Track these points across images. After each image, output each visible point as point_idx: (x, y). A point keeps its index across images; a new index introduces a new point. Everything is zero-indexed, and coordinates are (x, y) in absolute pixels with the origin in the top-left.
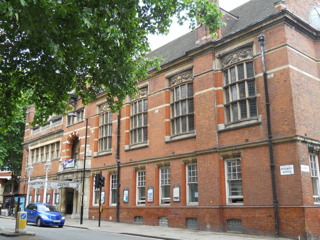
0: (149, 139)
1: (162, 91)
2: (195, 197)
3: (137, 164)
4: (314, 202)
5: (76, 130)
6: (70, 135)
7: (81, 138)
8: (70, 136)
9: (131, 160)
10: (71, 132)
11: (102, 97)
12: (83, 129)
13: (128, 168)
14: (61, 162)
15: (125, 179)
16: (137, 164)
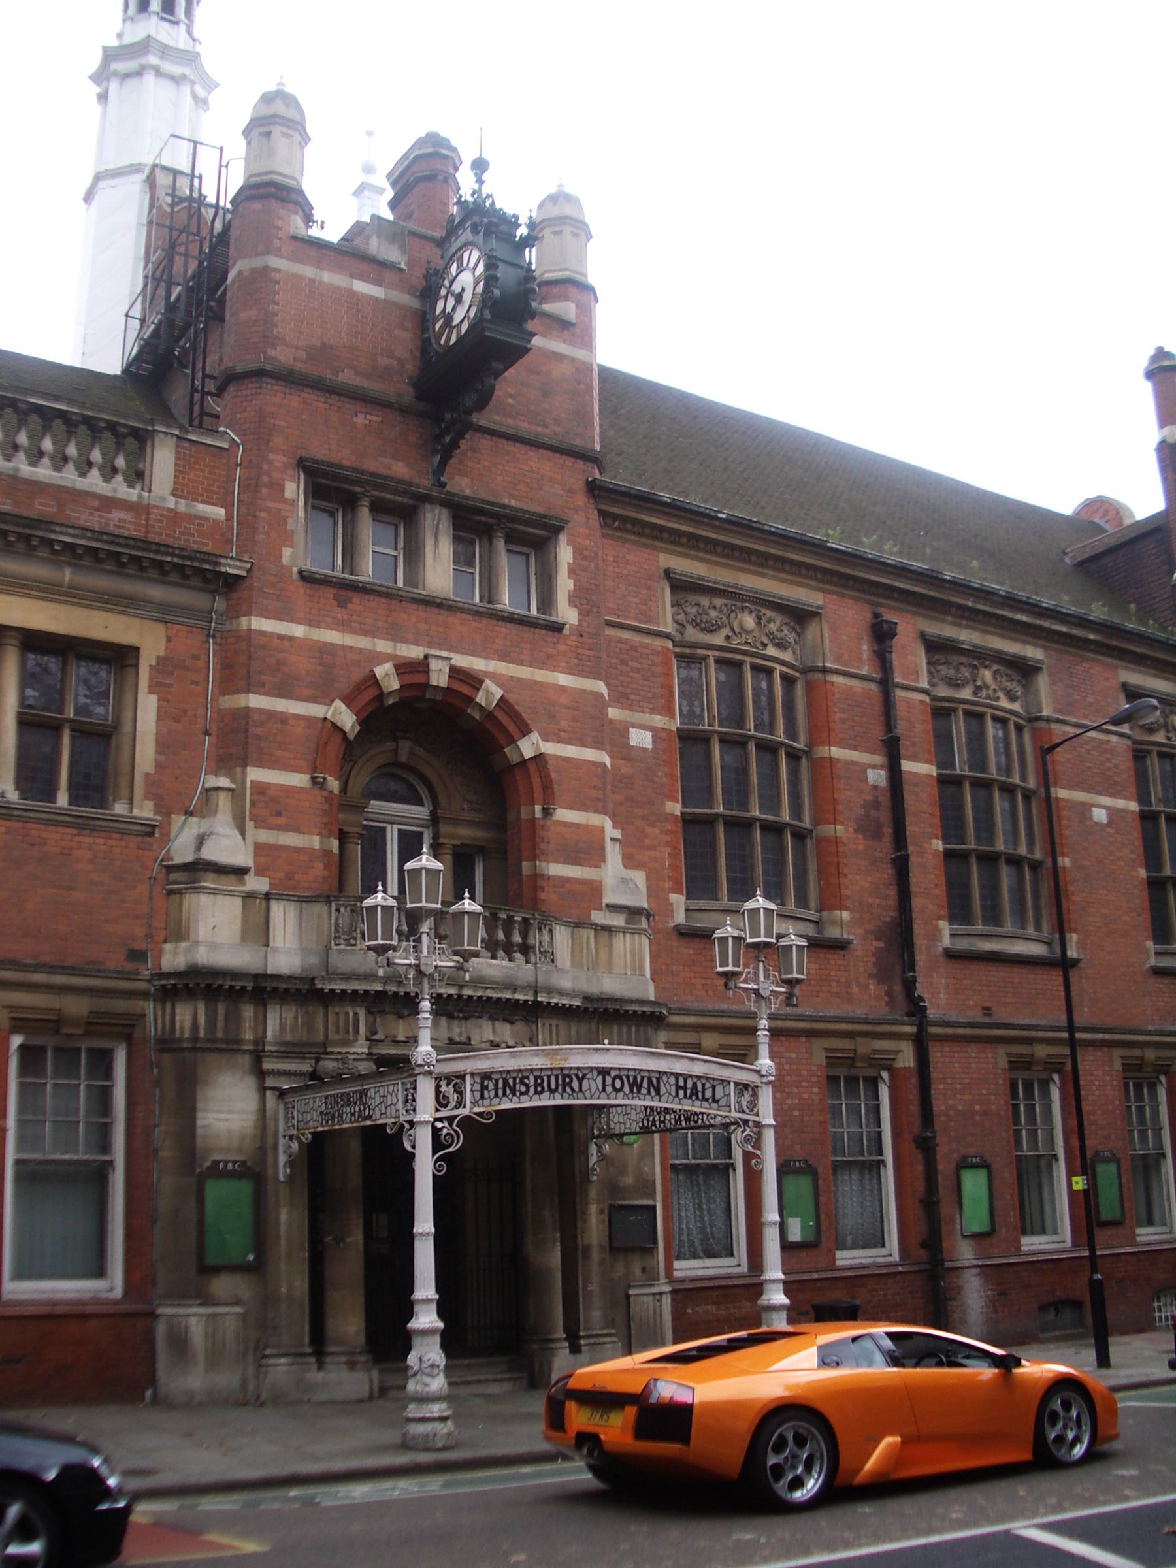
0: (1075, 931)
1: (1114, 738)
2: (798, 1220)
3: (1030, 1041)
4: (839, 1254)
5: (463, 661)
6: (388, 667)
7: (549, 748)
8: (387, 677)
9: (987, 1011)
10: (414, 652)
11: (742, 550)
12: (564, 689)
13: (972, 1051)
14: (240, 872)
15: (960, 1108)
16: (1030, 1041)
